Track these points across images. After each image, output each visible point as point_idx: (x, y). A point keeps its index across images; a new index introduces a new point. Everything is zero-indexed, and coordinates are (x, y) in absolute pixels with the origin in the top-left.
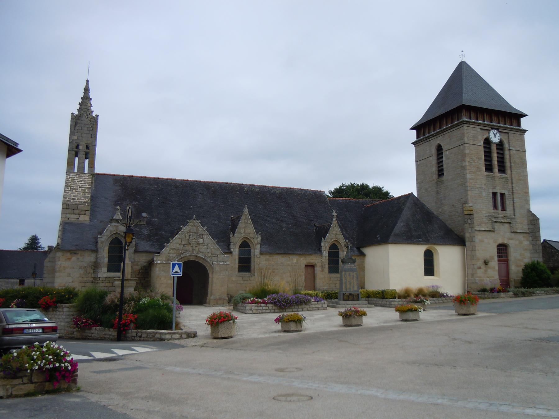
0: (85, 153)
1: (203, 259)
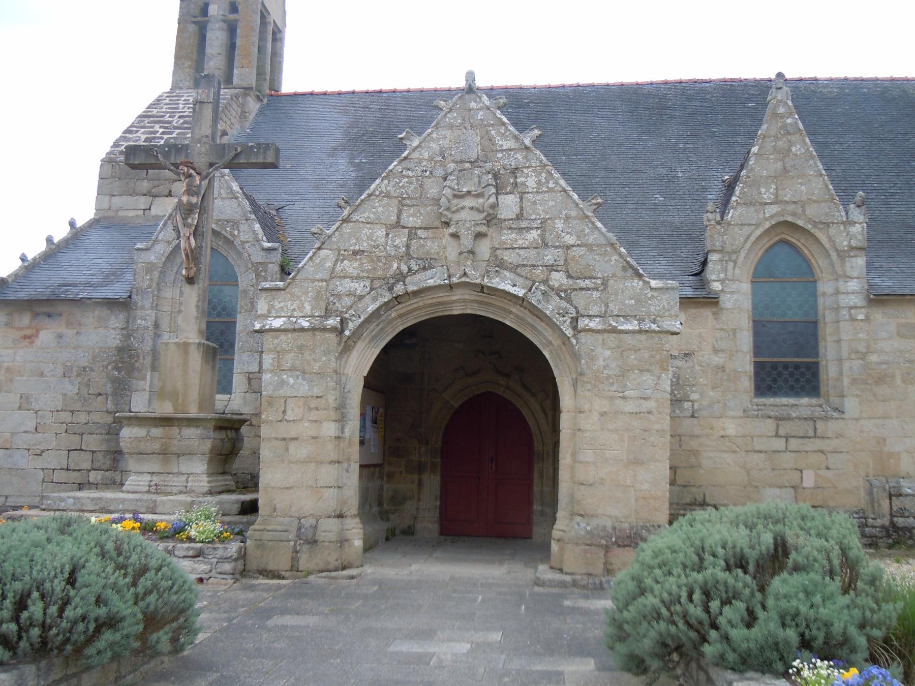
0: (225, 26)
1: (521, 301)
